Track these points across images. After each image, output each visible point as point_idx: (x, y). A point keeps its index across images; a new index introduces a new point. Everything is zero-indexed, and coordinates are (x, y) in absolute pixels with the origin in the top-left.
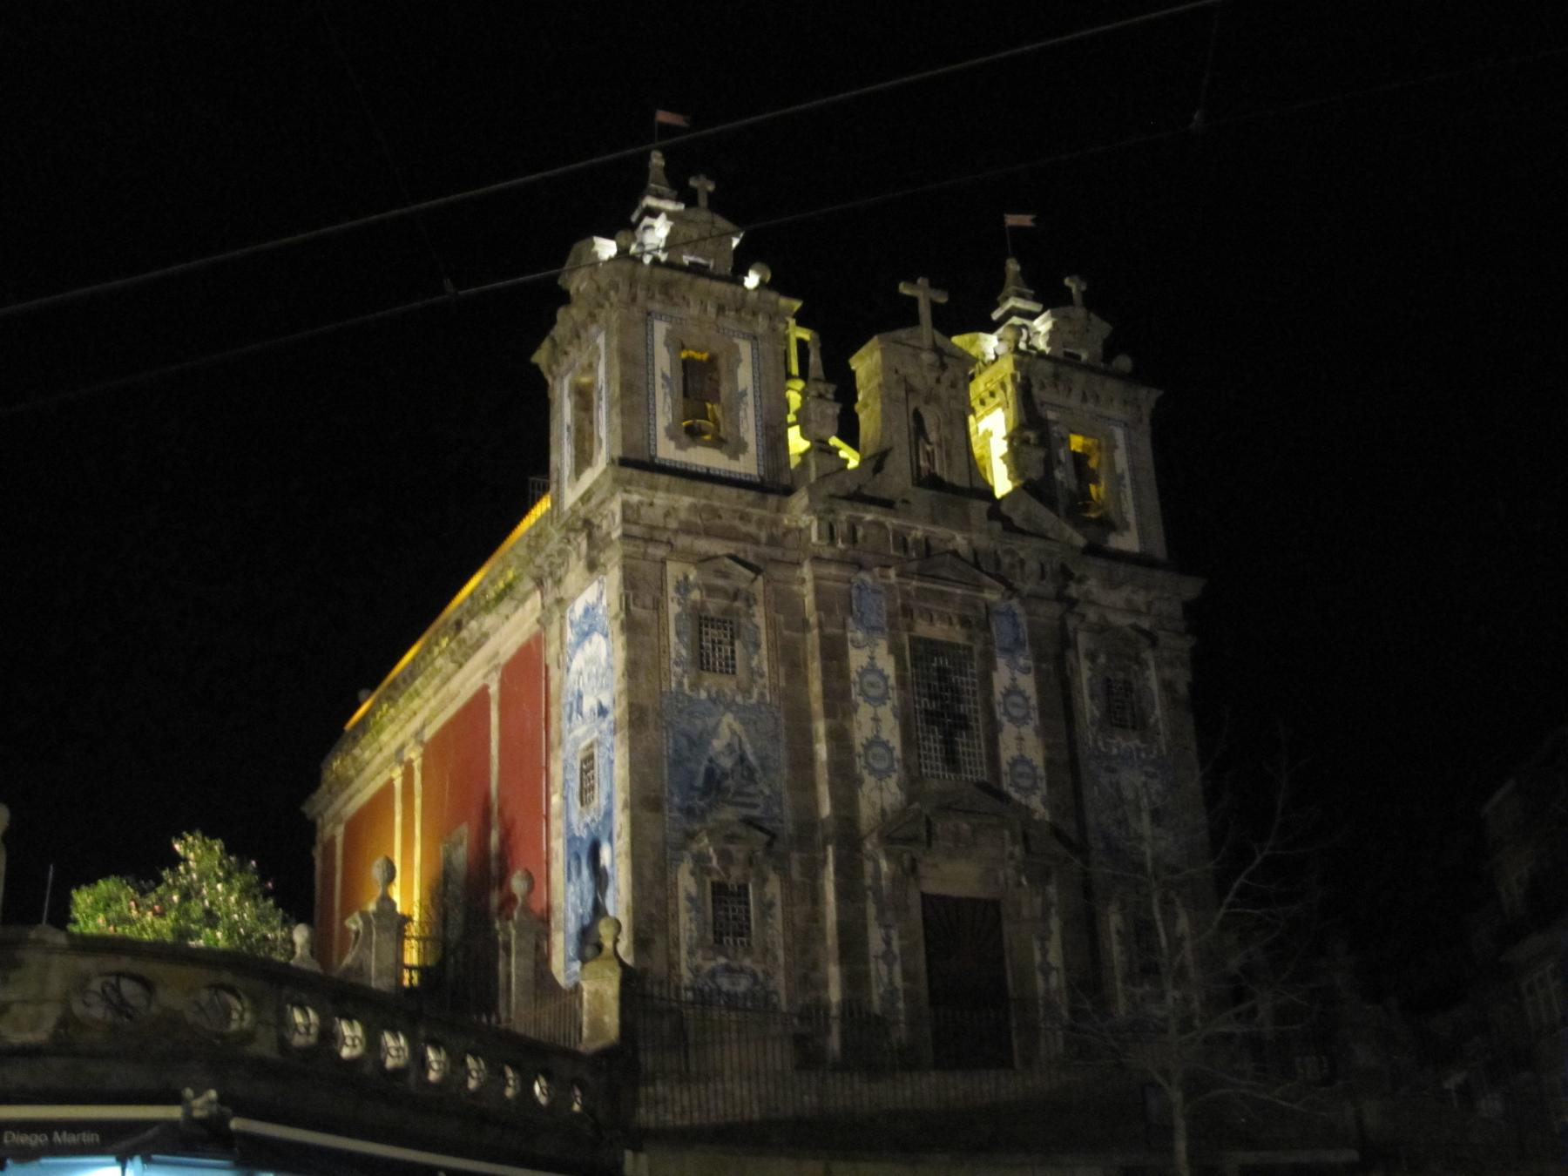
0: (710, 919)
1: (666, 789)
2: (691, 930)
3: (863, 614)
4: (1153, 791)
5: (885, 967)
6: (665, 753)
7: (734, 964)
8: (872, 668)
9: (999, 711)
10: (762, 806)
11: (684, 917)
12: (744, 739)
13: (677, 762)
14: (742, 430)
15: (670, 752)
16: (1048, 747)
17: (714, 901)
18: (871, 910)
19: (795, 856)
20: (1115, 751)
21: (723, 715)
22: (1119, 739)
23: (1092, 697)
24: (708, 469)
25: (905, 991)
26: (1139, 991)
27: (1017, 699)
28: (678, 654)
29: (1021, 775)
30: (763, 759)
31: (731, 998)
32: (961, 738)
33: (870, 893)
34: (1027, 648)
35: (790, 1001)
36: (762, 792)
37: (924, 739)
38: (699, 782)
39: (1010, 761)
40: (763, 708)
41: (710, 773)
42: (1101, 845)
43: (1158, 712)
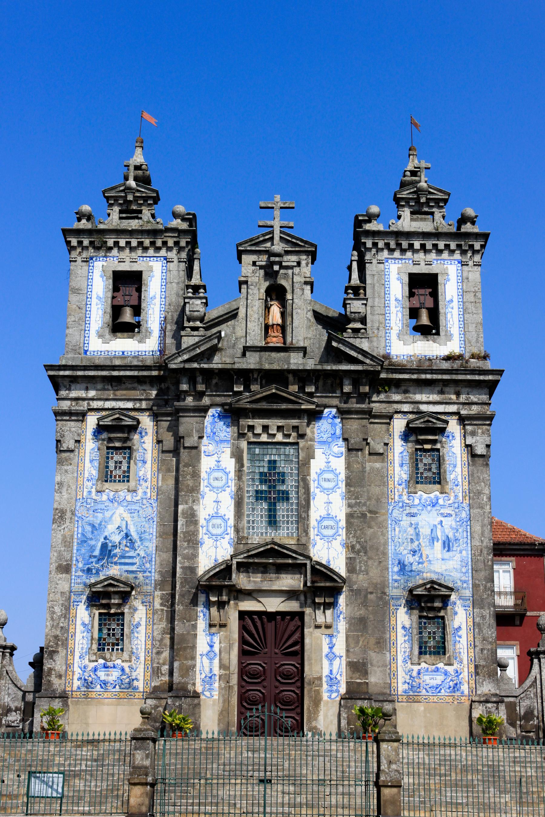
0: (96, 635)
1: (75, 559)
2: (82, 644)
3: (215, 433)
4: (445, 527)
5: (208, 661)
6: (76, 537)
7: (110, 664)
8: (218, 469)
9: (313, 486)
10: (138, 564)
11: (79, 636)
12: (129, 522)
13: (83, 541)
14: (149, 322)
15: (79, 536)
16: (349, 506)
17: (100, 625)
18: (202, 624)
19: (158, 593)
20: (417, 502)
21: (116, 509)
22: (420, 493)
23: (402, 465)
24: (123, 353)
25: (220, 676)
26: (416, 668)
27: (330, 476)
28: (90, 474)
29: (326, 527)
30: (141, 534)
31: (105, 683)
32: (282, 508)
33: (201, 615)
34: (341, 439)
35: (146, 683)
36: (139, 555)
37: (253, 510)
38: (97, 553)
39: (319, 519)
40: (145, 501)
41: (104, 546)
42: (396, 569)
43: (458, 469)
